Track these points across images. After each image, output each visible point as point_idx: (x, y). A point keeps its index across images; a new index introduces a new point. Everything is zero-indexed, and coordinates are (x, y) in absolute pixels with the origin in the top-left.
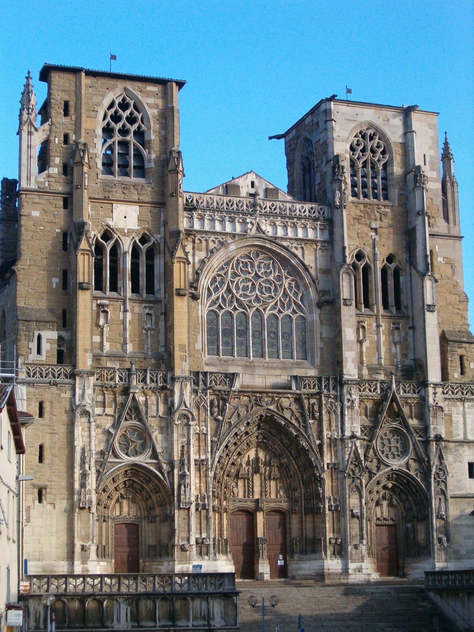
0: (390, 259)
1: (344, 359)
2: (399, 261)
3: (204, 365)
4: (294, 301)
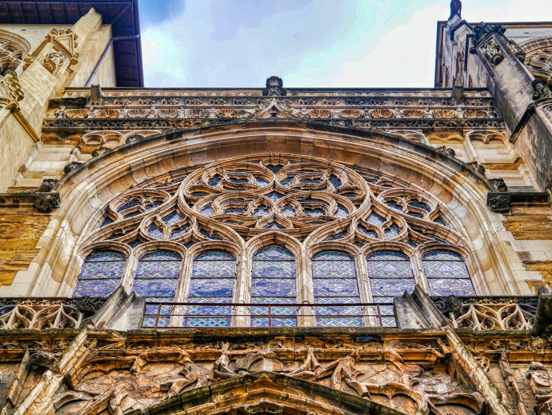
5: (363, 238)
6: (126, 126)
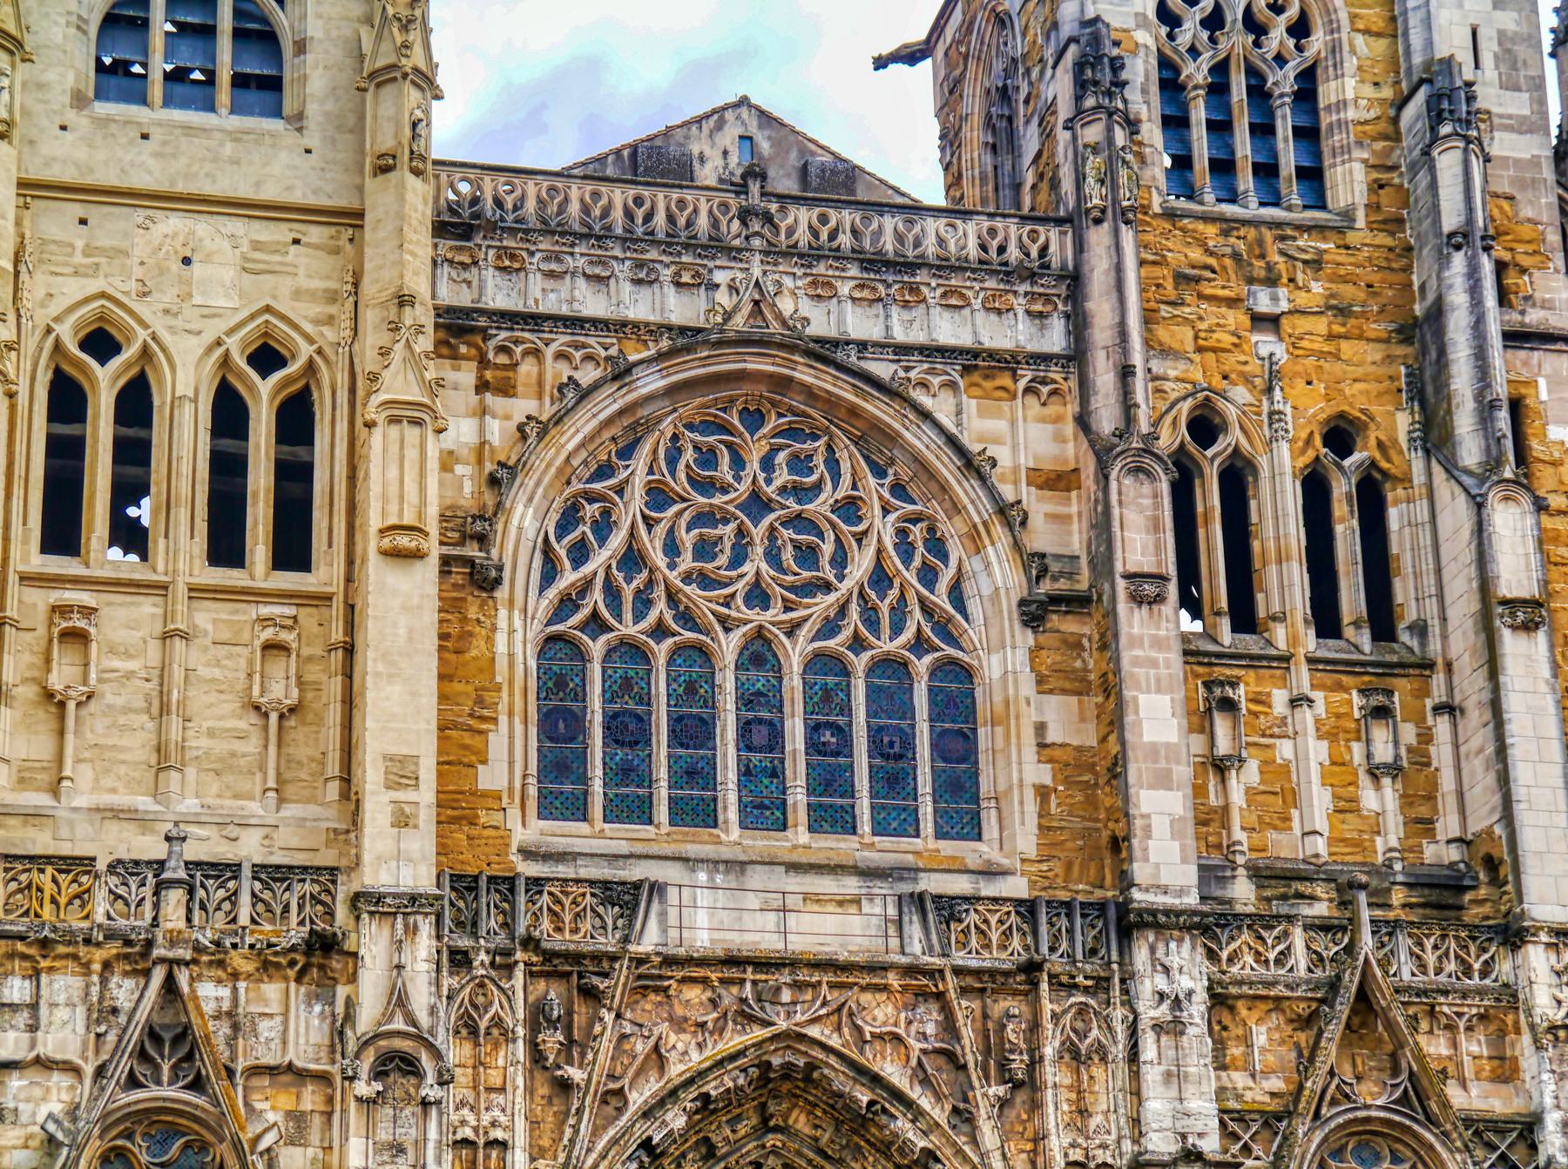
0: (1340, 436)
1: (1138, 823)
2: (1380, 445)
3: (515, 858)
4: (922, 602)
6: (547, 326)
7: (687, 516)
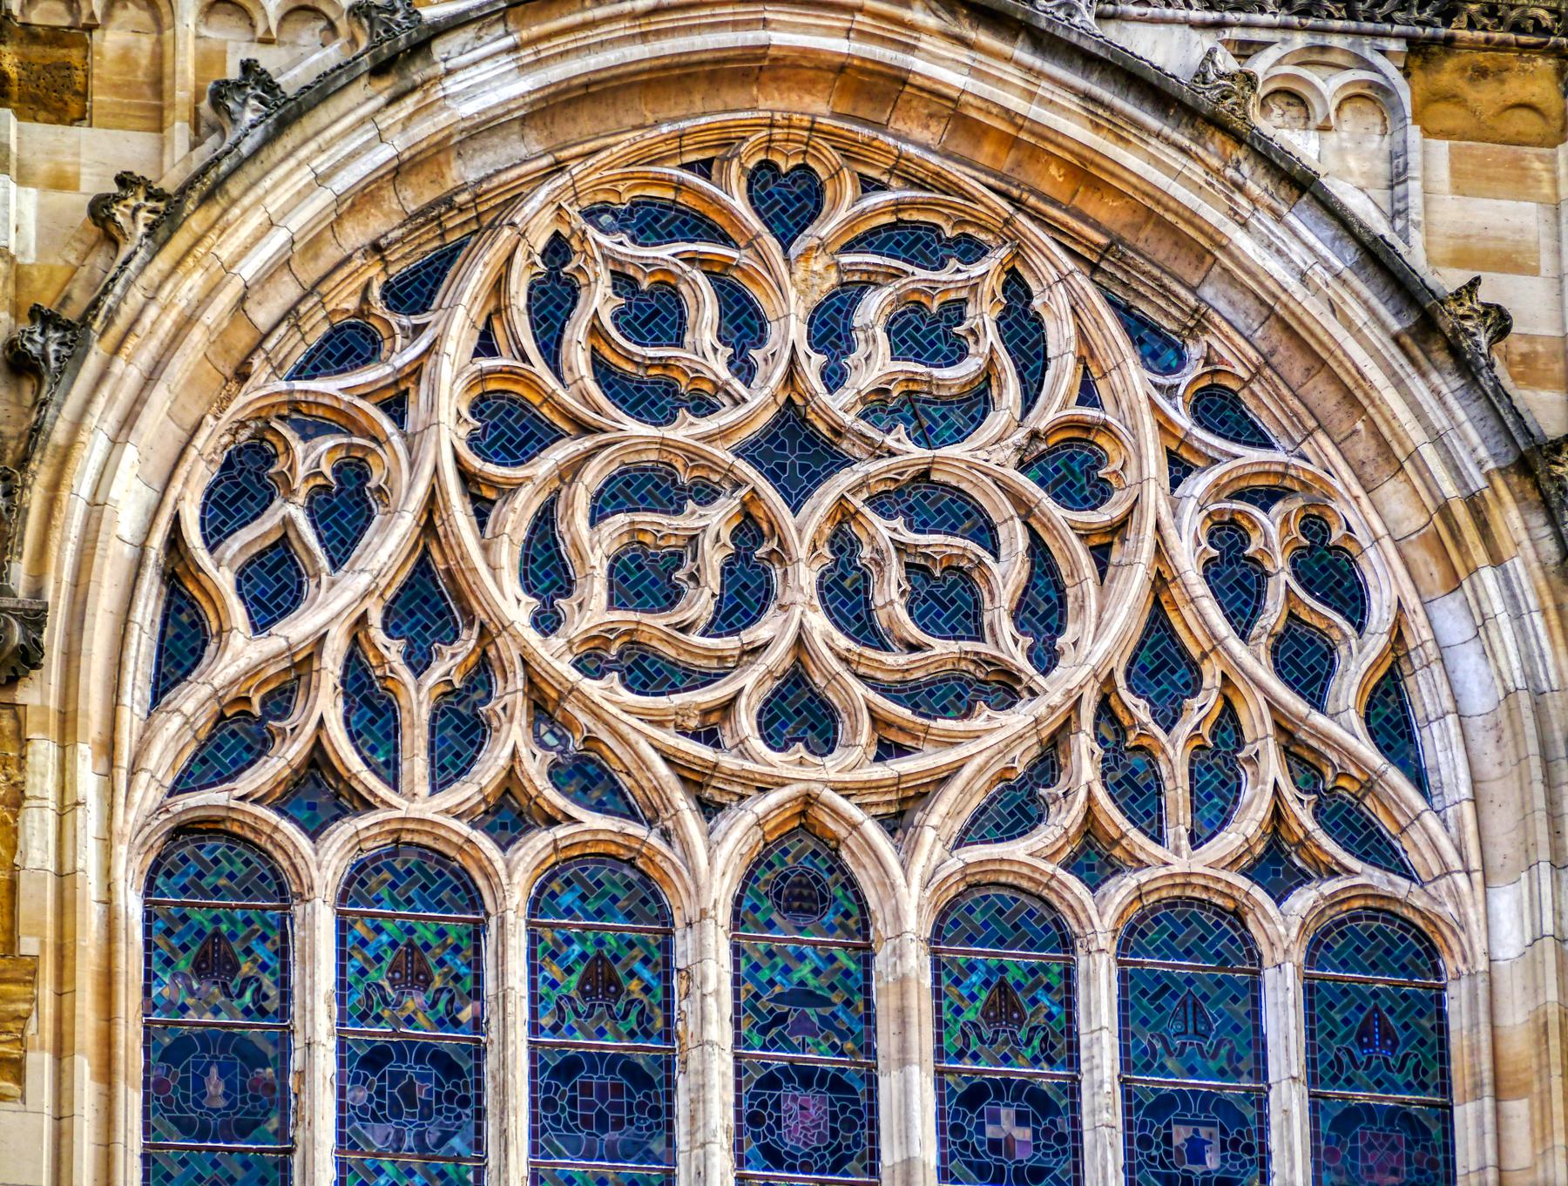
5: (1115, 834)
7: (593, 476)
